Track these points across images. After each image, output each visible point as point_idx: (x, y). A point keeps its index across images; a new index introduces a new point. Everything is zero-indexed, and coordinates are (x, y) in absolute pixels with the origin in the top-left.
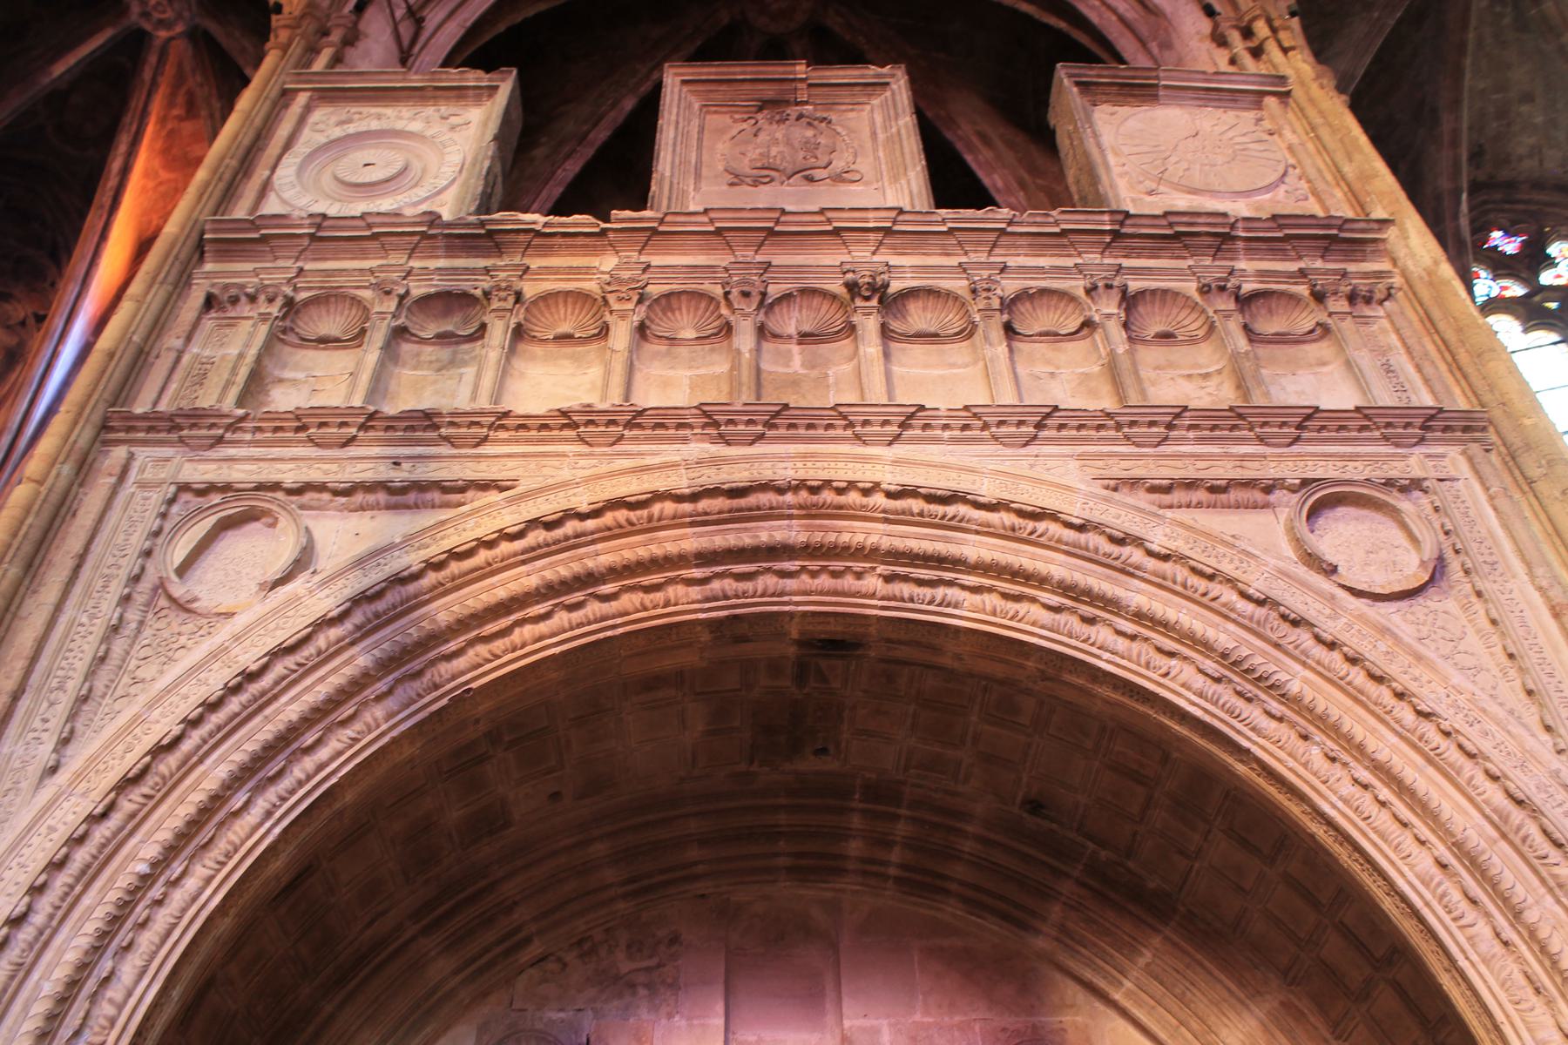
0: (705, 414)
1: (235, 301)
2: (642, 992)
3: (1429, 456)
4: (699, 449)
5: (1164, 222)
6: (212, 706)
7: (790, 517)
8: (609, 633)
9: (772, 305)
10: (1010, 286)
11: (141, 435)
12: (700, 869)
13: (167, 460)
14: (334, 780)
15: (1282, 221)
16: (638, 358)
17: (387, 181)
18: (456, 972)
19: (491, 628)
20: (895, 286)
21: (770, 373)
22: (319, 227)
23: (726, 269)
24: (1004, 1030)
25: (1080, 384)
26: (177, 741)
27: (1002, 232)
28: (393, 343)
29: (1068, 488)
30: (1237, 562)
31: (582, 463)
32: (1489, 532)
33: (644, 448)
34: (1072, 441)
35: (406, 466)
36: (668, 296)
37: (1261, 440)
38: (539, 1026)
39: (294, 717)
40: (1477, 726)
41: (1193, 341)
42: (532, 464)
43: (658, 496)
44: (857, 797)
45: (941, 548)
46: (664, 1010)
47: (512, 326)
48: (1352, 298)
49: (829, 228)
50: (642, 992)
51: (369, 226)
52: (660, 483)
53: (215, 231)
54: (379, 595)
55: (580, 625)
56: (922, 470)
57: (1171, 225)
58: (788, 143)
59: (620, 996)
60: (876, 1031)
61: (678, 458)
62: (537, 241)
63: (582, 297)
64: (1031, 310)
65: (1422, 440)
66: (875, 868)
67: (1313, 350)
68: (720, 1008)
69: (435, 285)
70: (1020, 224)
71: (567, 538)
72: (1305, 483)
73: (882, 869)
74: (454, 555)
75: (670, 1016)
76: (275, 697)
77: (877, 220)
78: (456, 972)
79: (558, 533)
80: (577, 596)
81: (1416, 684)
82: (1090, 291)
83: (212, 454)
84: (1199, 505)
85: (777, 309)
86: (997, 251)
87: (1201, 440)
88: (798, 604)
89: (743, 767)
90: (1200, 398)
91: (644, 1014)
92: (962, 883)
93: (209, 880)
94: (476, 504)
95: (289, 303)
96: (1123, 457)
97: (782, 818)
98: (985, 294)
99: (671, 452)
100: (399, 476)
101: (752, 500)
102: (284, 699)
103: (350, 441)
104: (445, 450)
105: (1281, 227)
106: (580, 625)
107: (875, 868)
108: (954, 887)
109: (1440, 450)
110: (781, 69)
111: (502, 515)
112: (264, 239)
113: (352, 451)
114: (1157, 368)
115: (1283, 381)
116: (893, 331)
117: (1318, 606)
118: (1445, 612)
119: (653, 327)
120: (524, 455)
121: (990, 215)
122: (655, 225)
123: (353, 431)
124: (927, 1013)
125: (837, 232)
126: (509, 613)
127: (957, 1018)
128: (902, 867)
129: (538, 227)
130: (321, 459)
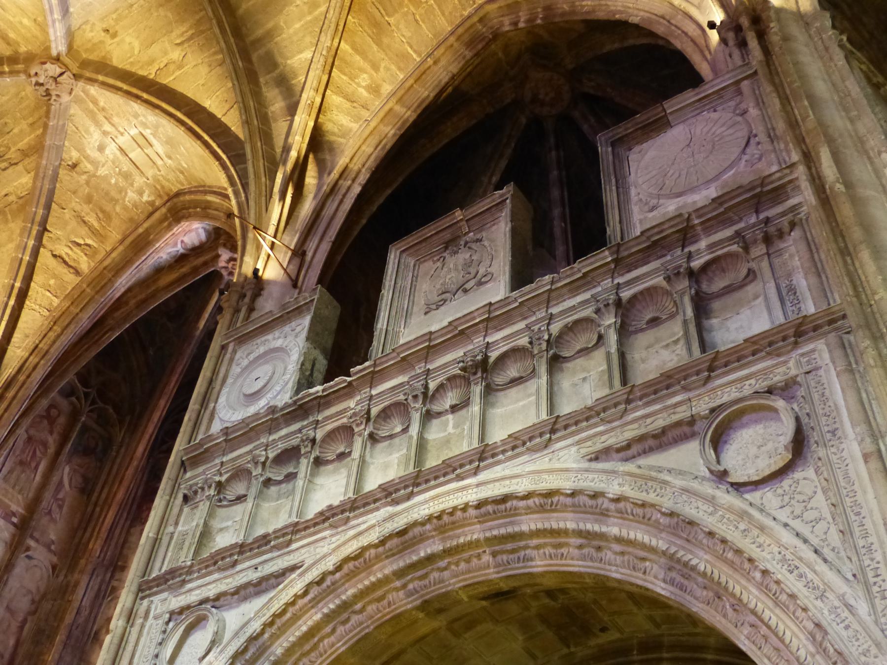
0: (384, 490)
1: (196, 492)
3: (802, 355)
5: (644, 238)
7: (433, 537)
8: (367, 631)
9: (433, 395)
11: (155, 589)
13: (166, 599)
15: (719, 201)
16: (371, 456)
17: (265, 386)
19: (307, 647)
20: (494, 355)
21: (435, 440)
22: (226, 434)
23: (408, 382)
25: (599, 380)
27: (550, 291)
28: (265, 490)
29: (567, 470)
30: (658, 490)
31: (334, 539)
32: (835, 405)
33: (361, 520)
34: (573, 434)
35: (260, 569)
36: (384, 410)
37: (685, 389)
40: (796, 572)
42: (312, 548)
43: (364, 549)
44: (635, 652)
47: (312, 460)
48: (768, 240)
49: (457, 332)
51: (248, 425)
52: (364, 541)
53: (186, 454)
54: (245, 650)
55: (351, 631)
56: (490, 486)
57: (648, 238)
58: (456, 269)
61: (373, 522)
62: (322, 401)
64: (573, 336)
65: (796, 344)
70: (560, 280)
71: (328, 587)
72: (712, 410)
74: (276, 616)
79: (324, 585)
80: (345, 616)
81: (759, 550)
82: (598, 311)
83: (183, 590)
85: (437, 395)
86: (551, 304)
87: (648, 404)
88: (454, 584)
89: (565, 651)
90: (671, 360)
94: (286, 582)
95: (219, 484)
96: (602, 433)
99: (372, 518)
103: (235, 564)
105: (721, 204)
106: (351, 631)
109: (811, 346)
110: (448, 219)
111: (295, 585)
112: (207, 450)
113: (239, 567)
114: (648, 348)
115: (729, 323)
116: (498, 385)
117: (705, 507)
118: (804, 479)
119: (379, 432)
121: (540, 284)
122: (372, 369)
123: (236, 557)
125: (462, 332)
126: (313, 636)
129: (320, 394)
130: (225, 578)
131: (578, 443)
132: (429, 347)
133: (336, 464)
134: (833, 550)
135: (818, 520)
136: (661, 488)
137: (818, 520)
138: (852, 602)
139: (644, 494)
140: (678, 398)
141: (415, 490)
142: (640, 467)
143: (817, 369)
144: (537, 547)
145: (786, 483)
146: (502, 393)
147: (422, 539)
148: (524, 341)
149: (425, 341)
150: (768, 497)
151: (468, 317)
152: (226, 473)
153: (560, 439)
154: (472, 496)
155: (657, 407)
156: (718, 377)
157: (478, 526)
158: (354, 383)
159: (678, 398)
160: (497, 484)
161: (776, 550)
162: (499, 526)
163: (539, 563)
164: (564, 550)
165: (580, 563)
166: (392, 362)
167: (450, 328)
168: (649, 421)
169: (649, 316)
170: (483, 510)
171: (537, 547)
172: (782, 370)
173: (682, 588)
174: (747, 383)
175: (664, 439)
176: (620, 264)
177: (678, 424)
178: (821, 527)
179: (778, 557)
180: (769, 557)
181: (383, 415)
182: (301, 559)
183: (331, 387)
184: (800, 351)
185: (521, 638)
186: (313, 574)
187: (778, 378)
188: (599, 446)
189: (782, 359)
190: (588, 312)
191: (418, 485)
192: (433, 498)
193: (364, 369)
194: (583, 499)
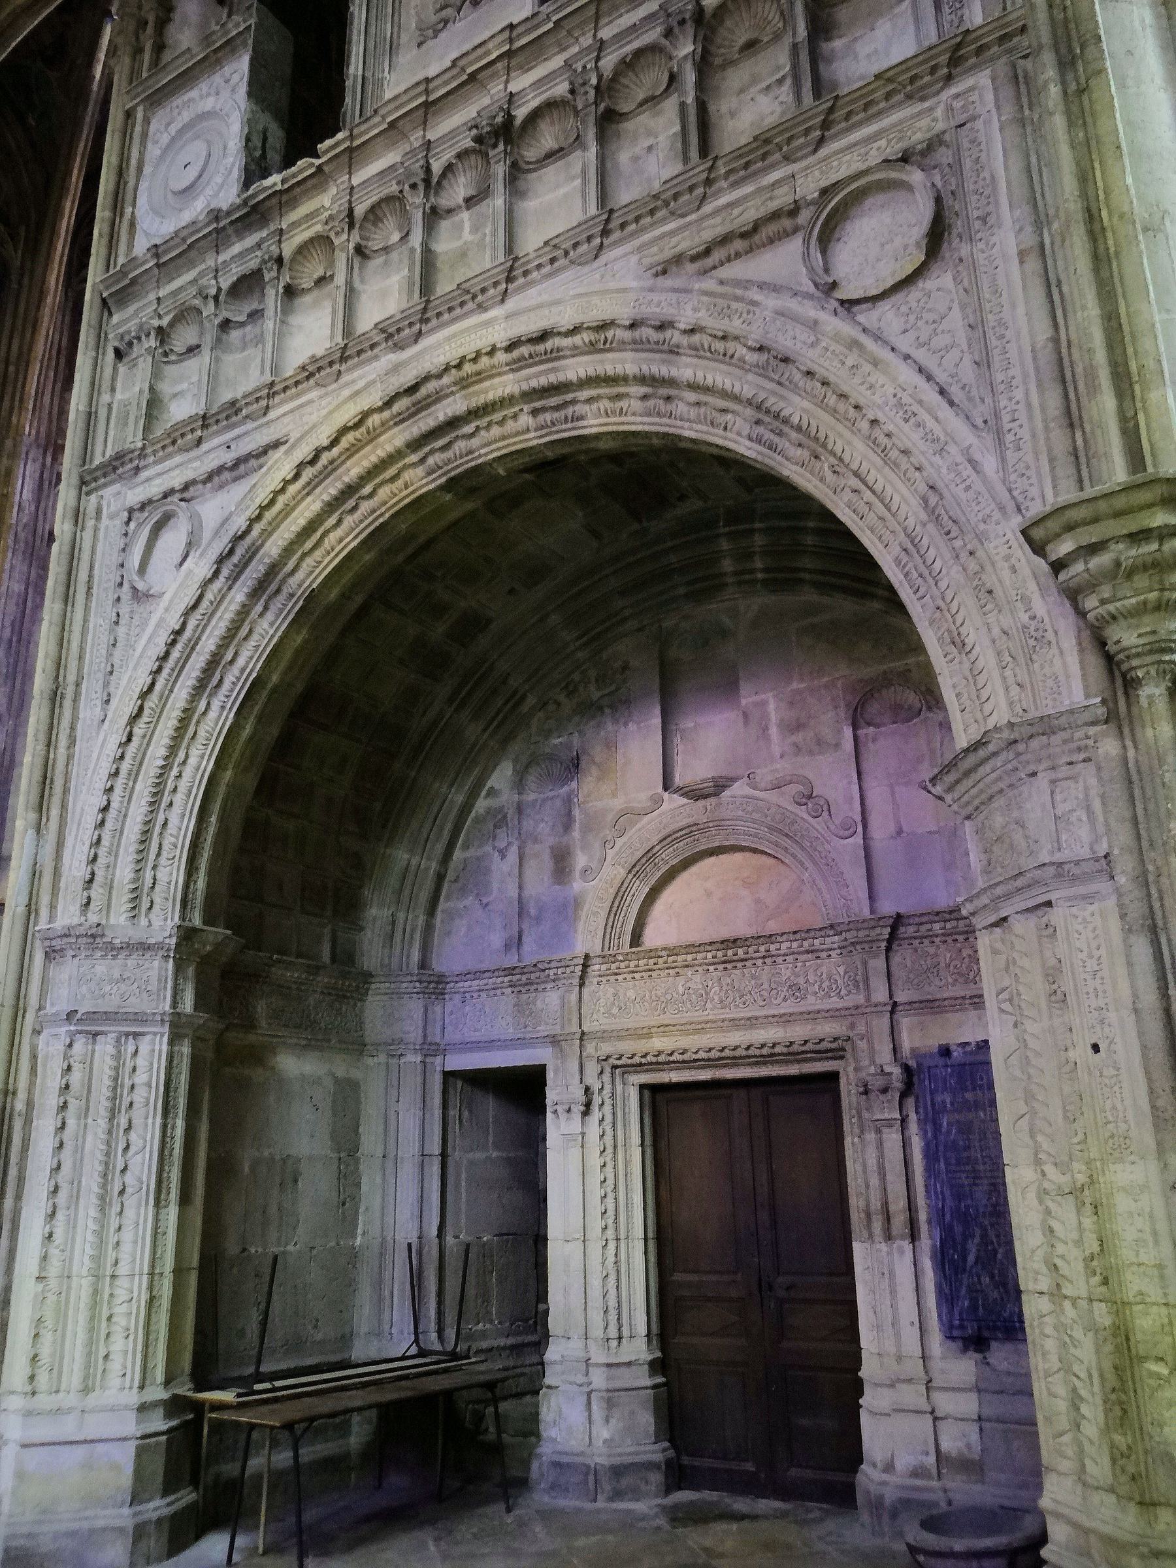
0: (383, 331)
1: (130, 344)
2: (607, 711)
3: (957, 96)
4: (390, 358)
6: (165, 657)
7: (452, 393)
8: (381, 520)
9: (439, 183)
11: (102, 481)
12: (627, 613)
13: (119, 493)
14: (254, 675)
16: (362, 281)
17: (200, 176)
18: (484, 730)
19: (309, 544)
20: (521, 113)
22: (157, 255)
24: (860, 681)
26: (153, 684)
28: (224, 336)
29: (624, 290)
31: (324, 403)
32: (993, 177)
33: (356, 374)
36: (373, 209)
37: (788, 159)
38: (547, 750)
39: (213, 648)
40: (912, 420)
43: (365, 415)
46: (622, 721)
47: (281, 290)
50: (607, 711)
51: (184, 240)
52: (364, 404)
53: (107, 288)
54: (231, 552)
55: (361, 521)
56: (524, 318)
59: (593, 717)
60: (764, 704)
62: (285, 198)
64: (634, 78)
66: (747, 577)
68: (657, 711)
71: (325, 467)
72: (824, 192)
73: (752, 577)
74: (263, 509)
75: (626, 724)
76: (199, 638)
77: (499, 46)
78: (484, 730)
79: (319, 465)
80: (351, 503)
82: (668, 33)
84: (738, 255)
85: (445, 183)
86: (603, 22)
87: (735, 185)
88: (486, 454)
91: (610, 727)
92: (811, 571)
93: (202, 757)
94: (270, 463)
95: (160, 330)
96: (672, 233)
97: (673, 558)
98: (582, 90)
101: (423, 391)
102: (204, 638)
103: (199, 441)
104: (250, 425)
106: (361, 521)
107: (747, 577)
108: (807, 576)
109: (969, 82)
111: (281, 466)
112: (134, 281)
113: (205, 446)
116: (528, 163)
117: (804, 336)
120: (292, 411)
122: (348, 144)
123: (199, 433)
124: (802, 680)
125: (473, 77)
126: (315, 531)
127: (825, 679)
128: (766, 570)
129: (279, 187)
130: (190, 461)
131: (640, 249)
132: (426, 105)
133: (315, 293)
134: (963, 388)
135: (948, 348)
136: (749, 312)
137: (948, 348)
138: (977, 456)
139: (726, 321)
141: (424, 328)
142: (721, 283)
143: (974, 118)
144: (590, 401)
145: (913, 295)
146: (534, 175)
147: (438, 397)
148: (561, 89)
149: (419, 94)
150: (886, 316)
151: (480, 51)
152: (166, 314)
153: (615, 243)
154: (500, 335)
155: (748, 189)
156: (835, 137)
157: (511, 376)
158: (326, 168)
160: (532, 315)
161: (890, 390)
162: (537, 375)
163: (592, 422)
164: (624, 404)
165: (646, 419)
166: (376, 131)
167: (455, 71)
168: (736, 212)
169: (741, 41)
170: (516, 354)
171: (590, 401)
172: (924, 123)
173: (772, 447)
174: (875, 145)
175: (756, 238)
177: (775, 216)
178: (952, 357)
179: (893, 401)
180: (880, 401)
181: (371, 217)
182: (284, 431)
183: (294, 176)
184: (953, 90)
185: (580, 514)
186: (303, 452)
187: (917, 136)
188: (668, 254)
189: (927, 104)
190: (653, 35)
191: (427, 321)
192: (449, 339)
193: (337, 144)
194: (646, 332)
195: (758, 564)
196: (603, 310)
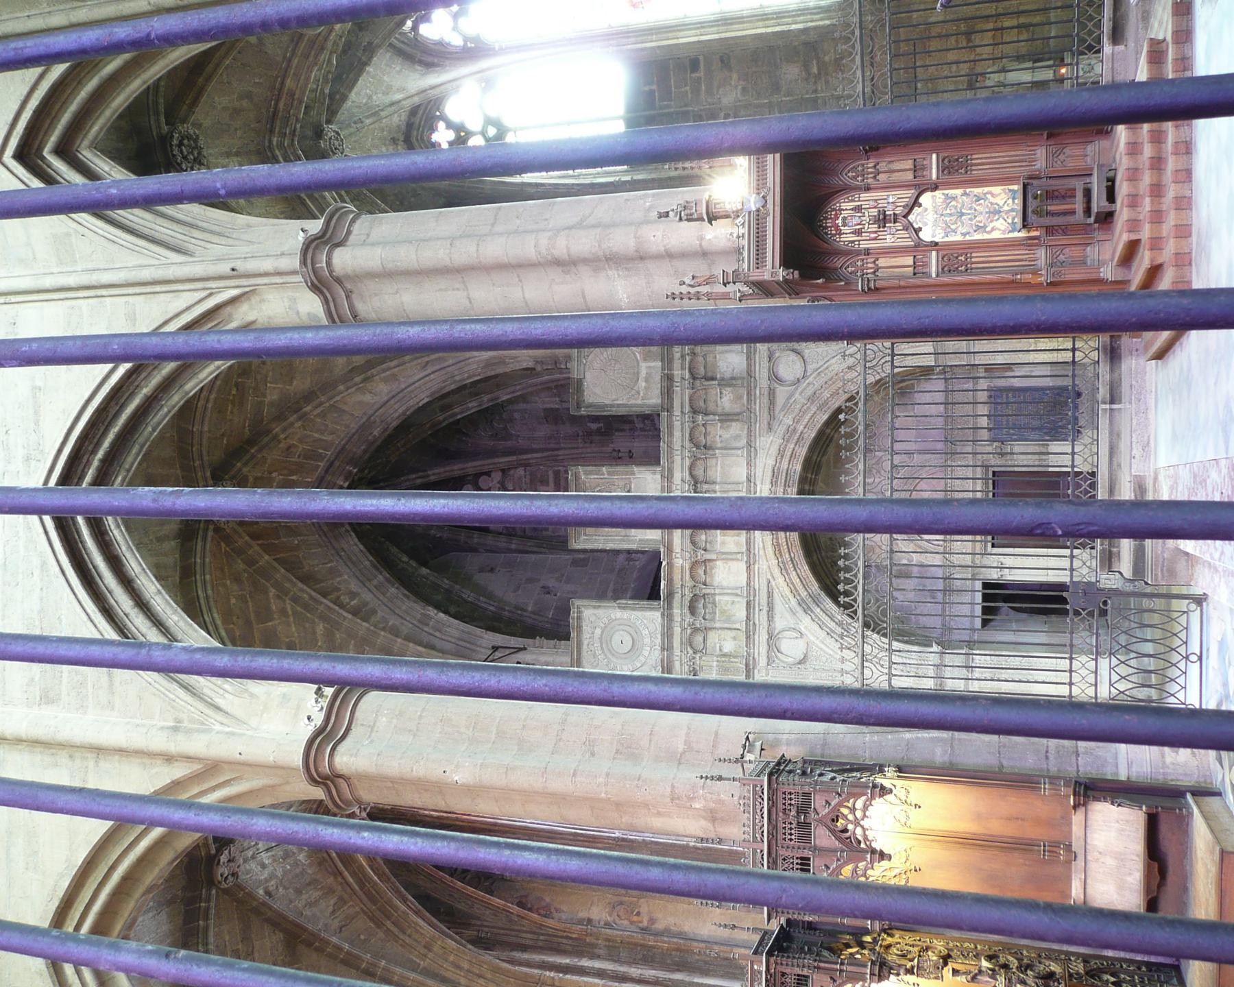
10: (687, 444)
41: (706, 394)
45: (784, 474)
63: (691, 569)
67: (710, 358)
69: (686, 610)
100: (765, 609)
104: (757, 598)
140: (758, 392)
150: (810, 368)
159: (758, 392)
176: (669, 410)
186: (776, 572)
188: (766, 426)
195: (809, 475)
196: (774, 450)
